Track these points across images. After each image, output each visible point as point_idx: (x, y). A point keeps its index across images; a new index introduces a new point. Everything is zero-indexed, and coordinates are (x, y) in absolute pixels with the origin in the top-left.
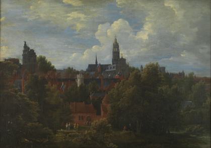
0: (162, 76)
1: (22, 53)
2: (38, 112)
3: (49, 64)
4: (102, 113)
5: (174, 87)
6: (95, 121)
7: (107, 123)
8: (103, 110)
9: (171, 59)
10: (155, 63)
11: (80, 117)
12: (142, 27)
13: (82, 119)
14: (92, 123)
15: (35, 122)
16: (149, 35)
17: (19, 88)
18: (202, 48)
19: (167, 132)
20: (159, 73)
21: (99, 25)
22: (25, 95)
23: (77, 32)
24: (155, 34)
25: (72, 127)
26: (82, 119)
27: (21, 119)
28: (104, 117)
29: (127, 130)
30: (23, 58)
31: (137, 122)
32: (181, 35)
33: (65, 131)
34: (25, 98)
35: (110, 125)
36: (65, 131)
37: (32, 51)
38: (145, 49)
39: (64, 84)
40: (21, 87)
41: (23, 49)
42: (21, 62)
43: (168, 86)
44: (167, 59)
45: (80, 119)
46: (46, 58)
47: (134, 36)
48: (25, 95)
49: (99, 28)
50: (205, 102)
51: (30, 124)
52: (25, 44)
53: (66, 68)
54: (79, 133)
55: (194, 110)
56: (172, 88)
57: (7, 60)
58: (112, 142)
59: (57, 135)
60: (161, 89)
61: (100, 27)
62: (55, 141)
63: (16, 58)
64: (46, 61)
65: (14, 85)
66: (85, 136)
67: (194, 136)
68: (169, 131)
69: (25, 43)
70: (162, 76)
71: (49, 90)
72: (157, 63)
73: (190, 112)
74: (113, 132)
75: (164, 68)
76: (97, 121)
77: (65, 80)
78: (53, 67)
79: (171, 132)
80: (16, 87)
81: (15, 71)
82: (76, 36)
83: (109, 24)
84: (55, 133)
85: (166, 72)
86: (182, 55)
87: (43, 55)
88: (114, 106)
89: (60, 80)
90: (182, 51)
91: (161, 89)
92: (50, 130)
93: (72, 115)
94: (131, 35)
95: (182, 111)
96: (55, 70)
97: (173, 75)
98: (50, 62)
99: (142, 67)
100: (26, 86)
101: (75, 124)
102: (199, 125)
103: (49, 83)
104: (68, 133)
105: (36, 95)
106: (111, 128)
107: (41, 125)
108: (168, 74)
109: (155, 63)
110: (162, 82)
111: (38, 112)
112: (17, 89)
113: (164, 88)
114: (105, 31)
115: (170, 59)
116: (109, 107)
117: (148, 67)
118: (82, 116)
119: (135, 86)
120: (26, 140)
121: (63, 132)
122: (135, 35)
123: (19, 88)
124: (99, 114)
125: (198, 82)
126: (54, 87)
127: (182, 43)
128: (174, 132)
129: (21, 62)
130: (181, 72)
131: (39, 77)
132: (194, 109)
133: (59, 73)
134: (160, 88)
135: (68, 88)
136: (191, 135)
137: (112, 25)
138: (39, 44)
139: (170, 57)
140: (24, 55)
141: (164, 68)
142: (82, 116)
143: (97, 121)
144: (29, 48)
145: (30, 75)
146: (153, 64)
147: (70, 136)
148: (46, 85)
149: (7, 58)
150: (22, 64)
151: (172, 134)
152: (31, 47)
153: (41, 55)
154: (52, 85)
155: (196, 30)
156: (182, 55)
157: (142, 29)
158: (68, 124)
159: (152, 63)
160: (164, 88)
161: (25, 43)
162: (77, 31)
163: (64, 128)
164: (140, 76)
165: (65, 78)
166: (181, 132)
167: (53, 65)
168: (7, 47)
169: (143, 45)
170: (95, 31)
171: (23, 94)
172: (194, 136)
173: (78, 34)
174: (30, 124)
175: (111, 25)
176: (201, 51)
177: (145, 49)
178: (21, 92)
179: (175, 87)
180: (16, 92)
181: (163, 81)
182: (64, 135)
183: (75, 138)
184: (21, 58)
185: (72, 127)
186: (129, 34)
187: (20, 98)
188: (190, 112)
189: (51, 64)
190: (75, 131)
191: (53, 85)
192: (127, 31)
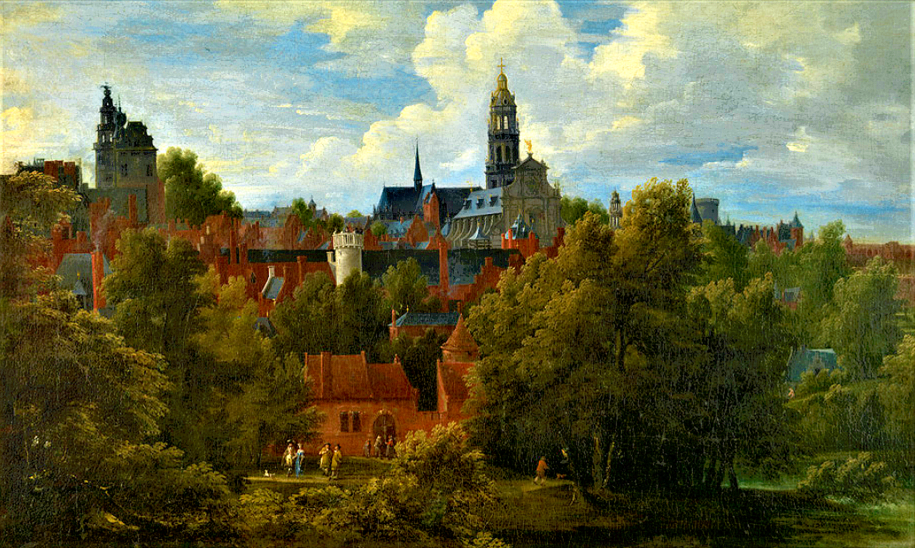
0: (706, 240)
1: (94, 138)
2: (163, 395)
3: (213, 187)
4: (443, 398)
5: (758, 286)
6: (410, 438)
7: (463, 445)
8: (448, 391)
9: (745, 163)
10: (674, 184)
11: (345, 417)
12: (616, 23)
13: (357, 428)
14: (399, 447)
15: (148, 440)
16: (647, 59)
17: (83, 293)
18: (881, 117)
19: (726, 484)
20: (691, 226)
21: (428, 15)
22: (109, 322)
23: (333, 46)
24: (674, 53)
25: (310, 464)
26: (357, 428)
27: (91, 428)
28: (450, 418)
29: (550, 474)
30: (99, 159)
31: (597, 438)
32: (787, 56)
33: (283, 479)
34: (109, 336)
35: (477, 454)
36: (283, 479)
37: (139, 128)
38: (630, 122)
39: (278, 273)
40: (87, 285)
41: (96, 119)
42: (89, 178)
43: (730, 281)
44: (724, 164)
45: (344, 429)
46: (199, 162)
47: (582, 62)
48: (109, 322)
49: (427, 29)
50: (892, 352)
51: (126, 450)
52: (108, 100)
53: (287, 202)
54: (341, 487)
55: (846, 389)
56: (748, 292)
57: (30, 169)
58: (488, 528)
59: (244, 498)
60: (702, 297)
61: (435, 21)
62: (238, 525)
63: (66, 160)
64: (200, 174)
65: (60, 278)
66: (369, 501)
67: (845, 500)
68: (734, 481)
69: (108, 92)
70: (706, 240)
71: (210, 300)
72: (684, 183)
73: (827, 396)
74: (492, 484)
75: (712, 205)
76: (421, 434)
77: (282, 257)
78: (230, 200)
79: (742, 486)
80: (71, 287)
81: (63, 217)
82: (331, 66)
83: (473, 11)
84: (238, 487)
85: (724, 223)
86: (791, 147)
87: (185, 148)
88: (496, 372)
89: (258, 258)
90: (795, 129)
91: (702, 297)
92: (217, 477)
93: (309, 411)
94: (570, 59)
95: (791, 393)
96: (238, 214)
97: (751, 234)
98: (213, 178)
99: (757, 227)
100: (111, 283)
101: (323, 451)
102: (865, 455)
103: (212, 268)
104: (296, 487)
105: (156, 320)
106: (481, 464)
107: (175, 452)
108: (730, 228)
109: (674, 184)
110: (703, 265)
111: (163, 395)
112: (71, 294)
113: (712, 291)
114: (456, 43)
115: (738, 165)
116: (472, 375)
117: (642, 201)
118: (356, 417)
119: (585, 284)
120: (111, 519)
121: (275, 487)
122: (589, 57)
123: (83, 293)
124: (428, 403)
125: (861, 264)
126: (236, 284)
127: (790, 94)
128: (759, 486)
129: (89, 178)
130: (788, 220)
131: (169, 244)
132: (844, 382)
133: (256, 227)
134: (693, 293)
135: (297, 290)
136: (832, 499)
137: (487, 14)
138: (167, 97)
139: (740, 157)
140: (102, 149)
141: (712, 205)
142: (356, 417)
143: (421, 434)
144: (122, 117)
145: (128, 233)
146: (665, 189)
147: (303, 501)
148: (196, 279)
149: (28, 161)
150: (92, 185)
151: (748, 492)
152: (133, 115)
153: (176, 146)
154: (224, 281)
155: (852, 35)
156: (791, 147)
157: (616, 31)
158: (296, 448)
159: (660, 180)
160: (712, 291)
161: (108, 92)
162: (335, 41)
163: (277, 466)
164: (608, 237)
165: (280, 247)
166: (789, 485)
167: (226, 189)
168: (27, 111)
169: (621, 104)
170: (411, 40)
171: (96, 316)
172: (845, 500)
173: (340, 55)
174: (126, 450)
175: (480, 15)
176: (875, 128)
177: (630, 122)
178: (89, 309)
179: (762, 287)
180: (65, 307)
181: (710, 261)
182: (278, 497)
183: (326, 512)
184: (91, 157)
185: (310, 464)
186: (559, 57)
187: (82, 337)
188: (827, 396)
189: (218, 187)
190: (323, 480)
191: (231, 279)
192: (551, 43)
